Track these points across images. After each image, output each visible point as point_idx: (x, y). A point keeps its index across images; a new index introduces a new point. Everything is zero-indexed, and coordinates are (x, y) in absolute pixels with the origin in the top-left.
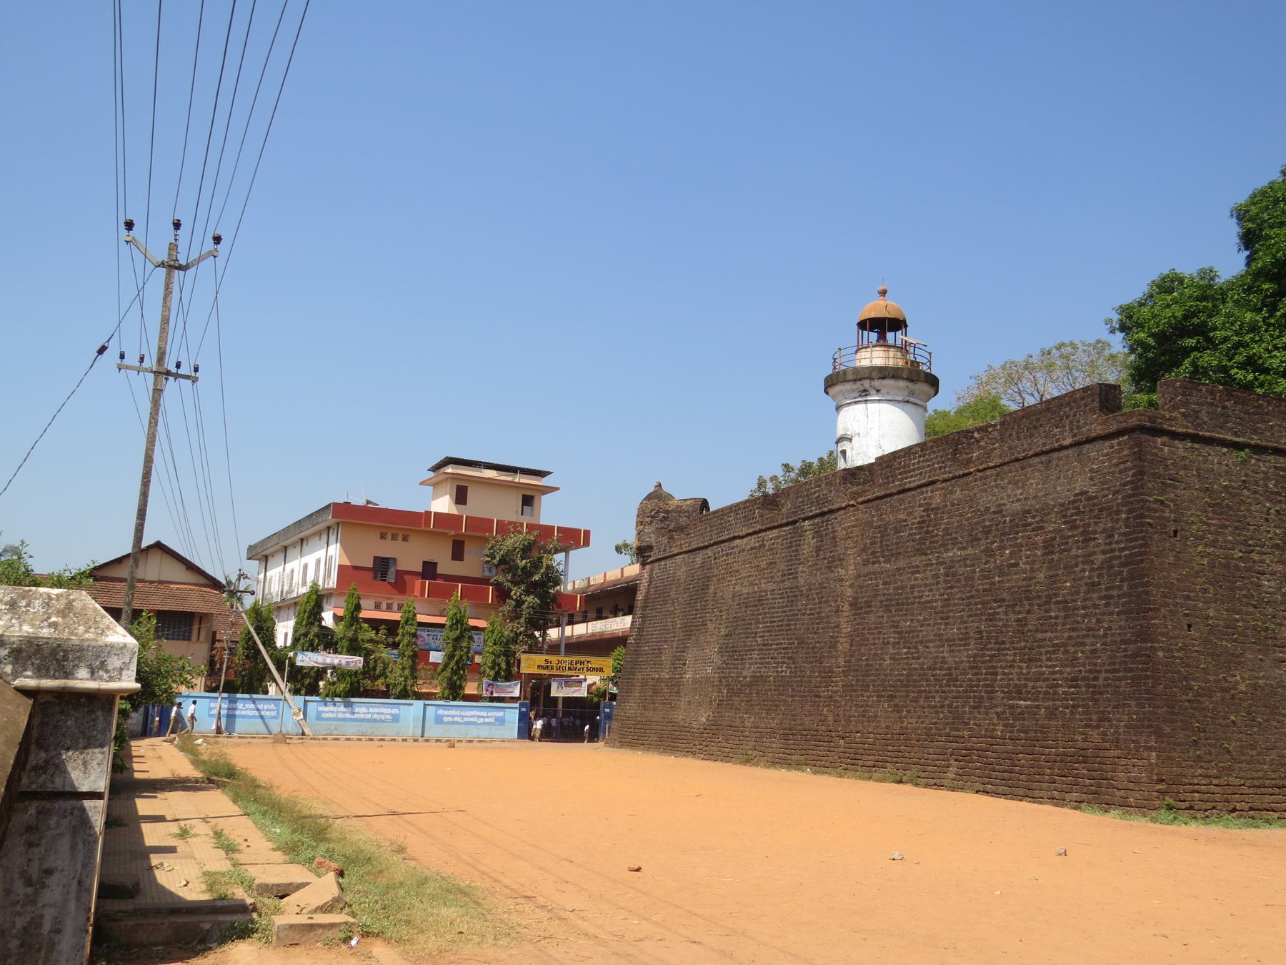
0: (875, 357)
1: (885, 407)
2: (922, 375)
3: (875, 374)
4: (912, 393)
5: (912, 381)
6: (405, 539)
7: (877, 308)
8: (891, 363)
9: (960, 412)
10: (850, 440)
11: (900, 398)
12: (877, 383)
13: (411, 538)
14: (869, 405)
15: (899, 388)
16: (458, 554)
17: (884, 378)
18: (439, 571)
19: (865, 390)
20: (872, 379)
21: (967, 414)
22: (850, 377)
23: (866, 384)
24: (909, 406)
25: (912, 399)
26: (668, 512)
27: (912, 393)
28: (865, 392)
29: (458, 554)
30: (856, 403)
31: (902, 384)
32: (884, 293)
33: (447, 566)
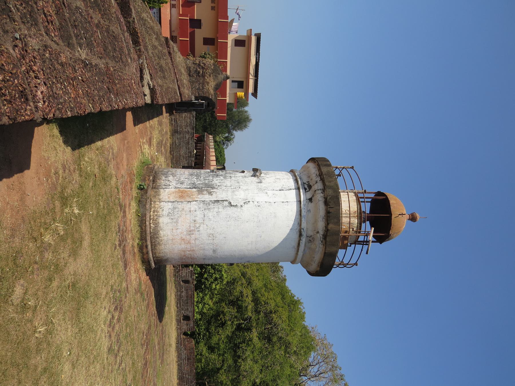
0: (348, 203)
1: (292, 210)
2: (333, 249)
3: (330, 192)
4: (311, 239)
5: (325, 236)
6: (213, 8)
7: (398, 207)
8: (345, 220)
9: (305, 327)
10: (254, 176)
11: (304, 225)
12: (319, 197)
13: (213, 12)
14: (294, 192)
15: (316, 222)
16: (207, 41)
17: (326, 203)
18: (197, 31)
19: (310, 187)
20: (324, 190)
21: (303, 331)
22: (324, 170)
23: (319, 186)
24: (296, 236)
25: (304, 239)
26: (203, 76)
27: (311, 239)
28: (308, 187)
29: (207, 41)
30: (296, 181)
31: (321, 225)
32: (413, 218)
33: (200, 35)
